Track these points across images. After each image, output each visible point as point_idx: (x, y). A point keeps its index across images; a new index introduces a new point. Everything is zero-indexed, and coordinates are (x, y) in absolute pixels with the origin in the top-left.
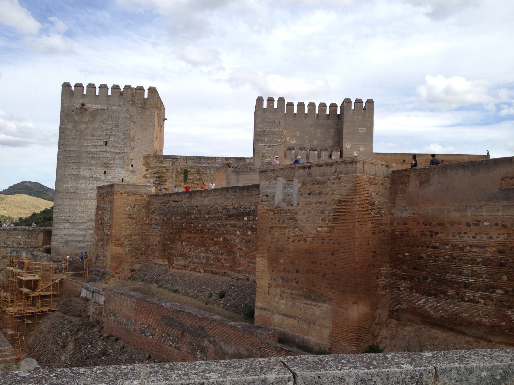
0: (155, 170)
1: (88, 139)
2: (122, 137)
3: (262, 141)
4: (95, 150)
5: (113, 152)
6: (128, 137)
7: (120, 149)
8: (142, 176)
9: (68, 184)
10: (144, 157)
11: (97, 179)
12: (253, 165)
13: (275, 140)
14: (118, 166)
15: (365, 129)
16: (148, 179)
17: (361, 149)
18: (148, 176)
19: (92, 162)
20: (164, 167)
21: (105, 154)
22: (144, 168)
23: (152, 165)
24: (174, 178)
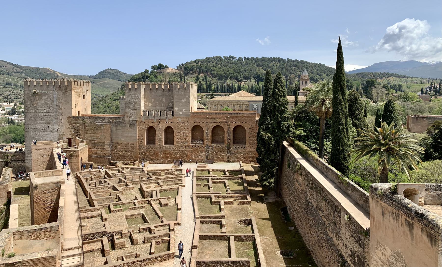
0: (74, 125)
1: (39, 109)
2: (56, 107)
3: (129, 108)
4: (43, 115)
5: (52, 116)
6: (59, 107)
7: (55, 114)
8: (67, 128)
9: (31, 133)
10: (67, 118)
11: (45, 131)
12: (124, 121)
13: (136, 106)
14: (55, 123)
15: (185, 99)
16: (70, 130)
17: (184, 111)
18: (70, 128)
19: (42, 121)
20: (78, 123)
21: (48, 117)
22: (68, 124)
23: (72, 122)
24: (84, 129)
